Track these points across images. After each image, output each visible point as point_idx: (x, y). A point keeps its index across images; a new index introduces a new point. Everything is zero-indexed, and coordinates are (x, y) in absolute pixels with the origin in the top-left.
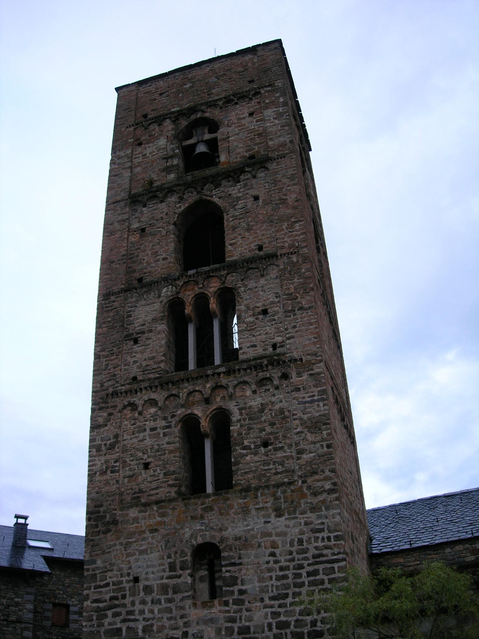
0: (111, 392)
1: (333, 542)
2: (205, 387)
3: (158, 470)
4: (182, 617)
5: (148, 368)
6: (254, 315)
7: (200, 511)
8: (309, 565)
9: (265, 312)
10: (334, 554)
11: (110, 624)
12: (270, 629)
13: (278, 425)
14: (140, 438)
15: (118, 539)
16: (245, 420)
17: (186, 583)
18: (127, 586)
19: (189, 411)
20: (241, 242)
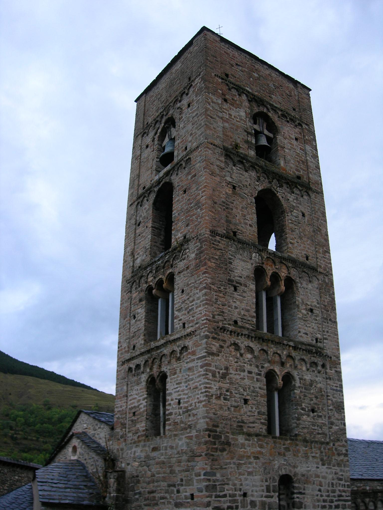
0: (221, 327)
2: (283, 353)
3: (254, 408)
7: (282, 450)
8: (336, 501)
14: (242, 376)
15: (232, 458)
18: (240, 499)
19: (272, 368)
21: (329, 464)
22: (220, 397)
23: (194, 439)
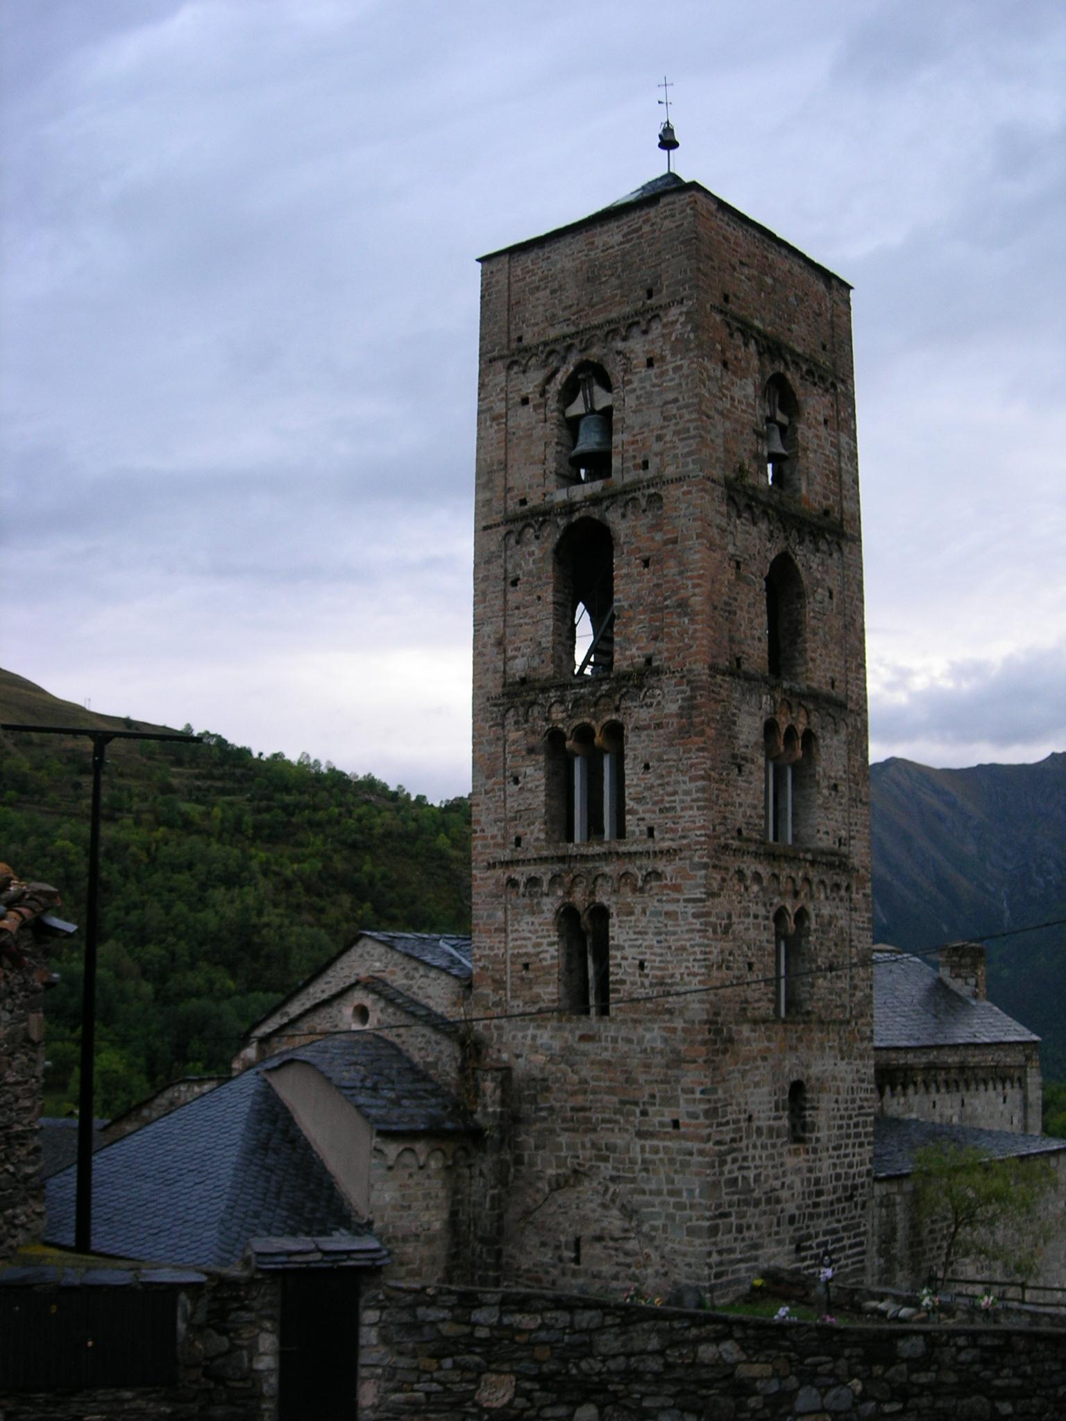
7: (794, 1042)
15: (736, 1064)
18: (743, 1125)
21: (850, 1058)
23: (679, 1033)
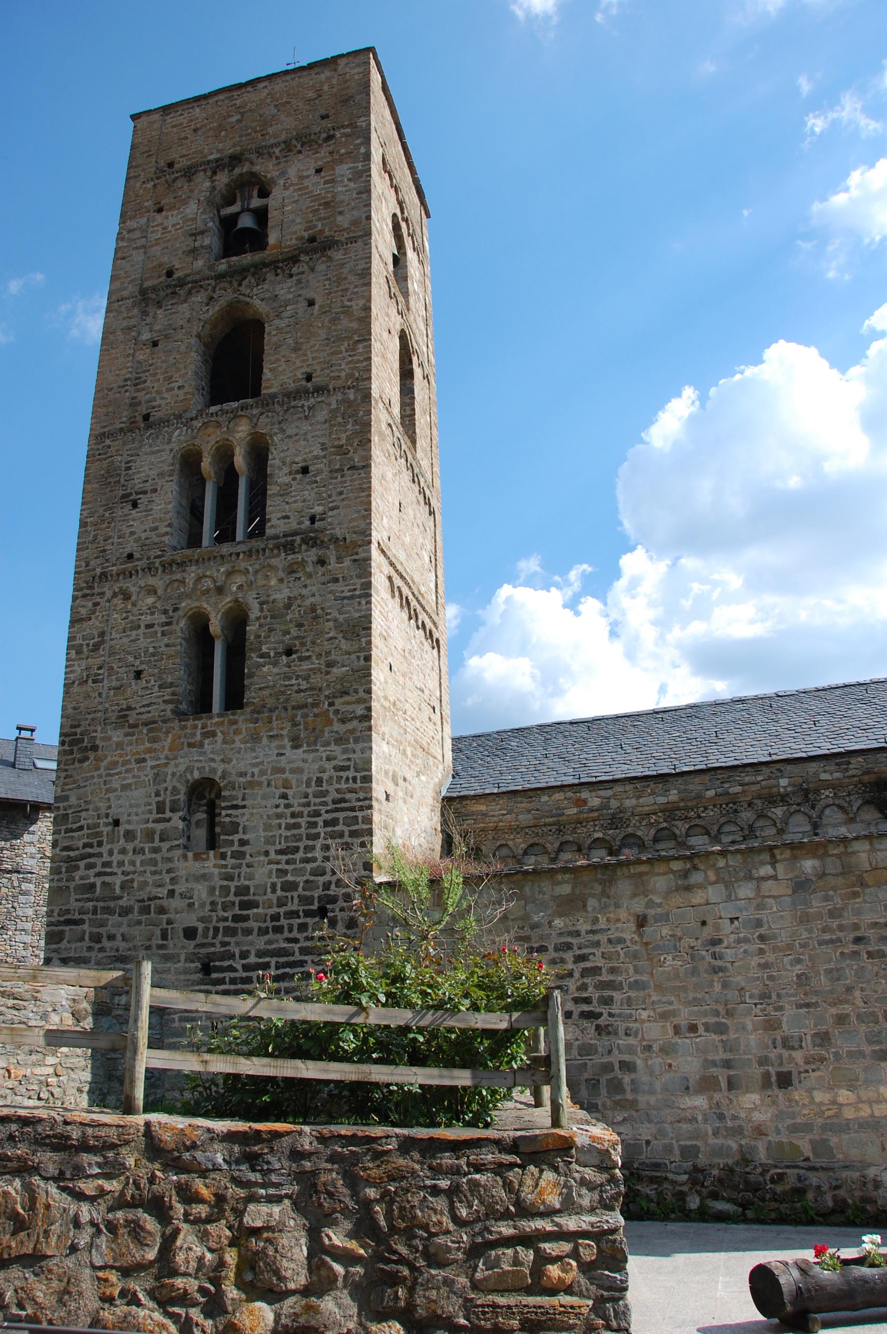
1: (359, 784)
2: (218, 571)
4: (169, 871)
5: (148, 542)
6: (290, 473)
7: (198, 737)
8: (327, 812)
9: (305, 470)
10: (359, 800)
11: (82, 878)
12: (274, 891)
13: (306, 627)
16: (265, 617)
17: (177, 828)
18: (105, 830)
20: (284, 366)
22: (86, 681)
